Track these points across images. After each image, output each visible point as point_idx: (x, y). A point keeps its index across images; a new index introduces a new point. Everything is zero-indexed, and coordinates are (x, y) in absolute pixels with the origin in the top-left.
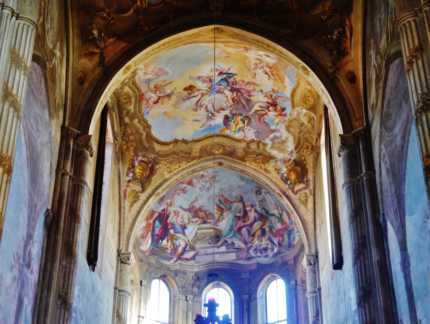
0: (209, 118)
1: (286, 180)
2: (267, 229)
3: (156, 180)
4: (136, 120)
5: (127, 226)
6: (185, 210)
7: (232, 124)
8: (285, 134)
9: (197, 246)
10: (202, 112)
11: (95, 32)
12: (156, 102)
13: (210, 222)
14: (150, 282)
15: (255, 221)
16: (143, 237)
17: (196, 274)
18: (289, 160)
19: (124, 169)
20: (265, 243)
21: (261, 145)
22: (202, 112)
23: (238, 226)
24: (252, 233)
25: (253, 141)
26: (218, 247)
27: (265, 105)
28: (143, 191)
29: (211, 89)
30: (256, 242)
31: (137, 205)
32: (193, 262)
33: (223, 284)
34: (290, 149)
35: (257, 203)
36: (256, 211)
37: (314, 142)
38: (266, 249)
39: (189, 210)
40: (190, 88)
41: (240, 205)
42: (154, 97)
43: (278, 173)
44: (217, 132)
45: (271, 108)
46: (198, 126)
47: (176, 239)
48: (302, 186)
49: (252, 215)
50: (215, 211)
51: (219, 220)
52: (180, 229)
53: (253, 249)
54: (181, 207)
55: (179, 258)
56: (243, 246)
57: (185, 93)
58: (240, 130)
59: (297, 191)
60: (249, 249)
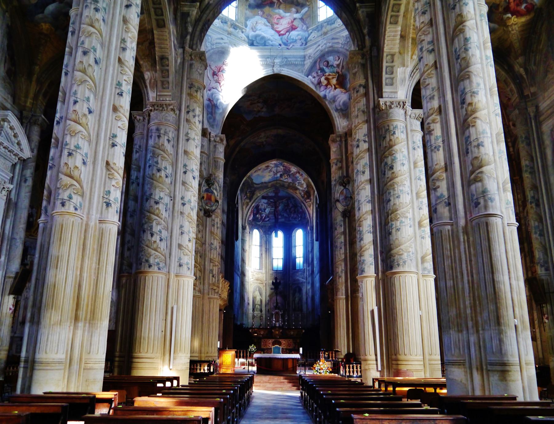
1: (303, 197)
3: (255, 197)
5: (245, 215)
8: (303, 182)
9: (270, 216)
10: (272, 173)
11: (236, 166)
14: (251, 229)
15: (292, 207)
16: (250, 215)
17: (270, 226)
19: (243, 195)
22: (272, 173)
25: (291, 183)
28: (250, 202)
31: (248, 207)
32: (268, 222)
40: (268, 167)
46: (270, 177)
48: (309, 200)
49: (291, 205)
52: (263, 210)
55: (263, 221)
56: (287, 216)
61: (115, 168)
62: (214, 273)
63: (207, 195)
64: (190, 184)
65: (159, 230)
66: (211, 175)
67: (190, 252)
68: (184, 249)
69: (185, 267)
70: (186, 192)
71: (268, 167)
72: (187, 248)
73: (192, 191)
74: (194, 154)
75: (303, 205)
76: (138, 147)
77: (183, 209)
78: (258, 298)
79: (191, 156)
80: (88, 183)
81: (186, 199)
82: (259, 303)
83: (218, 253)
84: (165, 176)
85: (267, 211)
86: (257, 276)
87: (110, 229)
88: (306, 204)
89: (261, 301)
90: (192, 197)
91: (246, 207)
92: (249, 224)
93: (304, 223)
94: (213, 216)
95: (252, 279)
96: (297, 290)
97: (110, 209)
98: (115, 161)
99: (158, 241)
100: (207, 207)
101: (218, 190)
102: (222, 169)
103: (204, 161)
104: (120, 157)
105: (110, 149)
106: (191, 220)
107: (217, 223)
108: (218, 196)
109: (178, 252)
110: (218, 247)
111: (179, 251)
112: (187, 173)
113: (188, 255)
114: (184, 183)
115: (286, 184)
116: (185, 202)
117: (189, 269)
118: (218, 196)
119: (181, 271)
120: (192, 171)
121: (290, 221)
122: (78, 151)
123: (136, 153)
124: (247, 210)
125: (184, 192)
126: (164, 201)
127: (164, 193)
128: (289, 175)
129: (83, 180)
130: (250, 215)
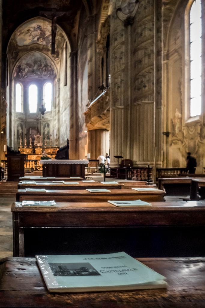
2: (47, 70)
6: (25, 64)
7: (40, 40)
10: (31, 37)
20: (46, 73)
21: (47, 47)
22: (31, 37)
23: (39, 68)
25: (45, 45)
26: (34, 74)
27: (49, 35)
29: (34, 30)
30: (44, 73)
32: (27, 79)
35: (44, 62)
36: (44, 64)
37: (62, 46)
39: (26, 64)
40: (29, 30)
41: (40, 62)
42: (19, 34)
44: (35, 42)
46: (30, 41)
49: (43, 65)
51: (34, 67)
54: (24, 64)
55: (23, 77)
57: (27, 32)
58: (41, 42)
59: (56, 60)
71: (29, 30)
75: (53, 63)
78: (21, 131)
88: (55, 62)
89: (22, 133)
93: (53, 76)
95: (16, 119)
121: (41, 77)
128: (44, 39)
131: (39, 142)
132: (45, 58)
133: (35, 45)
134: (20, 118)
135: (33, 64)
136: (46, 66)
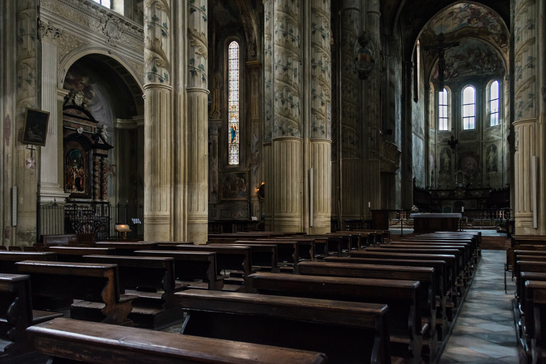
0: (461, 21)
1: (497, 42)
2: (491, 60)
4: (428, 31)
6: (453, 57)
8: (496, 23)
9: (459, 70)
11: (410, 20)
12: (436, 23)
13: (464, 60)
16: (435, 73)
18: (499, 34)
20: (489, 66)
21: (486, 29)
22: (457, 20)
23: (477, 59)
24: (484, 62)
25: (482, 27)
26: (469, 70)
33: (471, 85)
34: (499, 29)
36: (485, 53)
38: (490, 69)
41: (478, 51)
43: (494, 39)
44: (465, 26)
45: (489, 14)
46: (456, 26)
47: (450, 70)
48: (504, 45)
49: (484, 54)
50: (466, 55)
51: (468, 58)
53: (484, 69)
54: (451, 57)
55: (451, 77)
56: (480, 68)
58: (475, 23)
60: (483, 68)
61: (196, 34)
62: (373, 135)
63: (362, 56)
64: (320, 45)
65: (289, 96)
66: (364, 32)
67: (324, 116)
68: (317, 112)
69: (320, 131)
70: (316, 54)
72: (320, 111)
73: (322, 52)
74: (322, 10)
76: (268, 15)
77: (314, 73)
78: (447, 160)
79: (319, 13)
80: (171, 53)
81: (317, 62)
82: (448, 165)
83: (376, 115)
84: (292, 39)
85: (456, 65)
86: (445, 138)
87: (198, 97)
88: (502, 50)
90: (323, 58)
91: (429, 65)
92: (434, 83)
94: (369, 77)
95: (439, 142)
96: (492, 148)
97: (196, 77)
98: (195, 28)
99: (289, 108)
100: (362, 69)
101: (374, 49)
102: (377, 24)
103: (356, 19)
104: (200, 23)
105: (190, 16)
106: (322, 83)
107: (374, 84)
108: (373, 54)
109: (312, 116)
110: (376, 110)
111: (313, 115)
112: (316, 32)
113: (322, 119)
114: (313, 44)
115: (476, 30)
116: (316, 65)
117: (323, 132)
118: (373, 54)
119: (316, 135)
120: (322, 29)
121: (484, 72)
122: (156, 22)
123: (267, 21)
124: (430, 67)
125: (314, 53)
126: (292, 67)
127: (291, 58)
128: (479, 19)
129: (165, 51)
130: (435, 73)
131: (461, 182)
132: (486, 45)
133: (465, 29)
134: (445, 141)
135: (466, 55)
136: (489, 54)
